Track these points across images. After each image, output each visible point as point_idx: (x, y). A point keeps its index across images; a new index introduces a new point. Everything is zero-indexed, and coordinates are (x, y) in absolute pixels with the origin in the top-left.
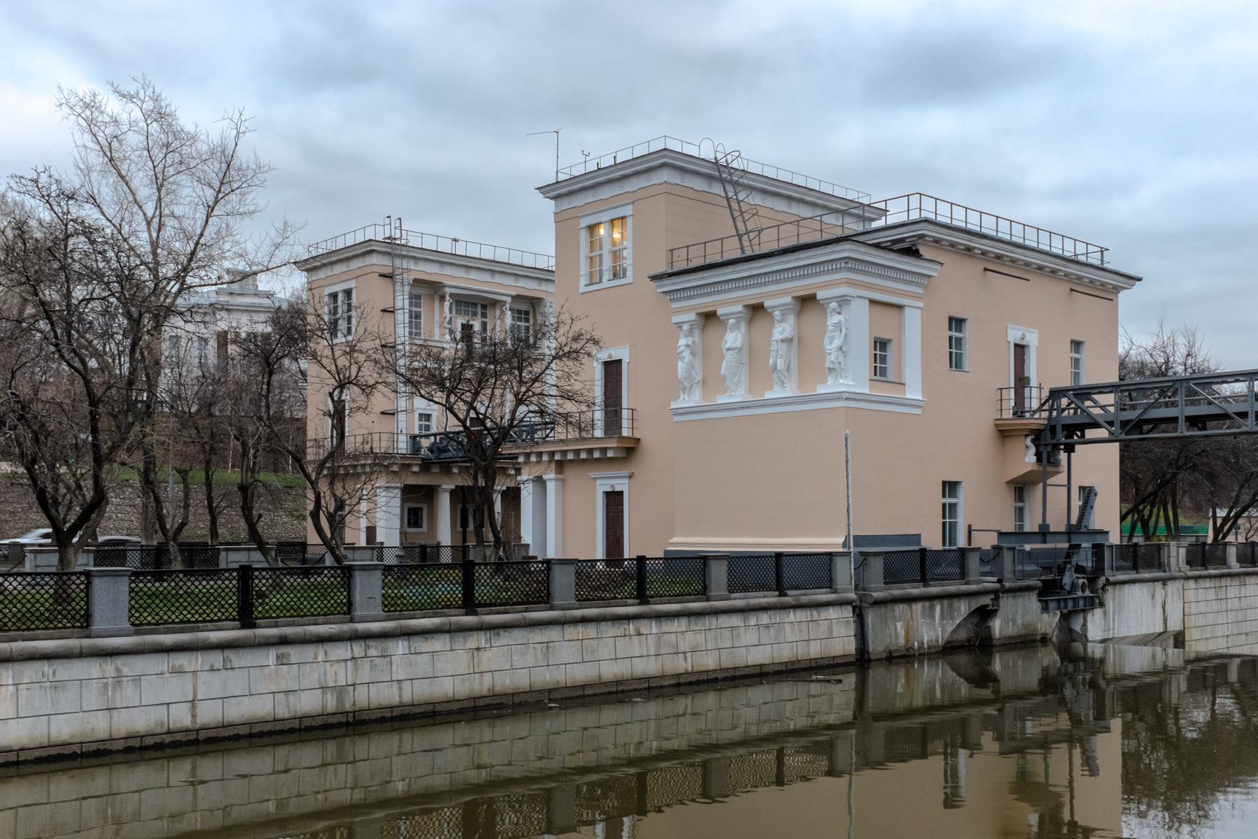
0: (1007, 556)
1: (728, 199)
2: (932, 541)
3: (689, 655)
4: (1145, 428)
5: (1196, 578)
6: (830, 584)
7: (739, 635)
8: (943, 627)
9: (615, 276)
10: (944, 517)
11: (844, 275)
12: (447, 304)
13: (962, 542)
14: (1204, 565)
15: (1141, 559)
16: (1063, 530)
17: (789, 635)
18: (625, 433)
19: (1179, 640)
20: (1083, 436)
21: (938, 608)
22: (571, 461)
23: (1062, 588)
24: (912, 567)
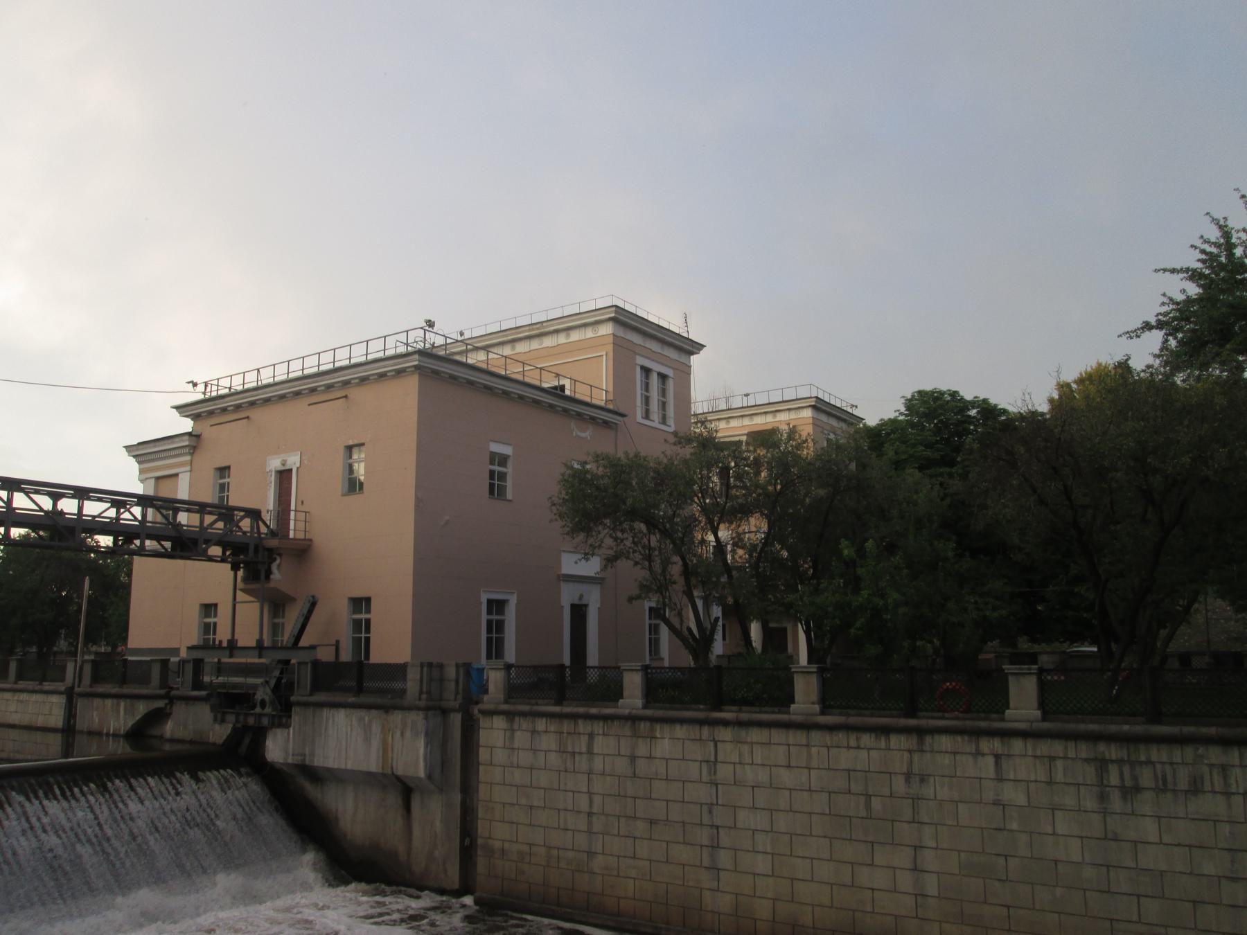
5: (510, 716)
16: (254, 644)
17: (12, 708)
21: (122, 704)
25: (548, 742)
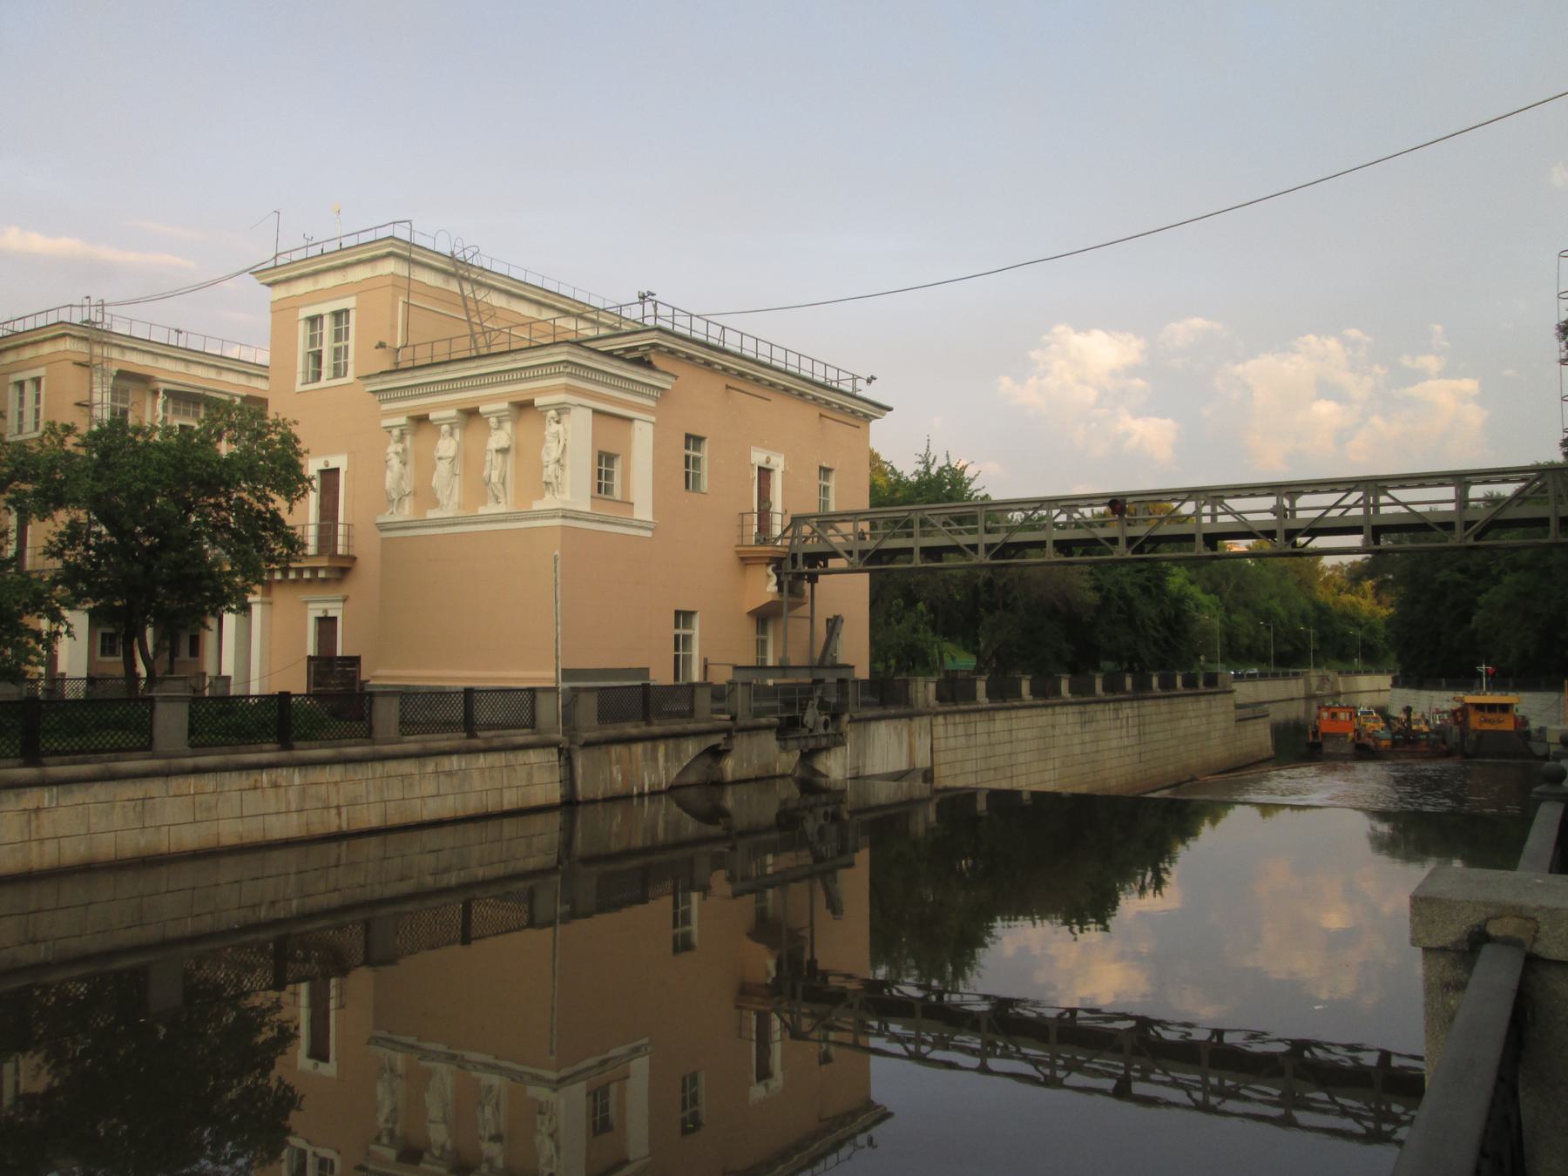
0: (741, 693)
1: (464, 298)
2: (662, 676)
3: (344, 810)
4: (885, 558)
5: (945, 714)
6: (532, 724)
7: (411, 785)
8: (667, 769)
9: (337, 375)
10: (677, 649)
11: (562, 380)
12: (160, 401)
13: (696, 676)
14: (954, 700)
15: (885, 694)
18: (340, 551)
19: (928, 775)
20: (826, 565)
22: (279, 582)
23: (804, 726)
24: (631, 706)
25: (961, 730)
